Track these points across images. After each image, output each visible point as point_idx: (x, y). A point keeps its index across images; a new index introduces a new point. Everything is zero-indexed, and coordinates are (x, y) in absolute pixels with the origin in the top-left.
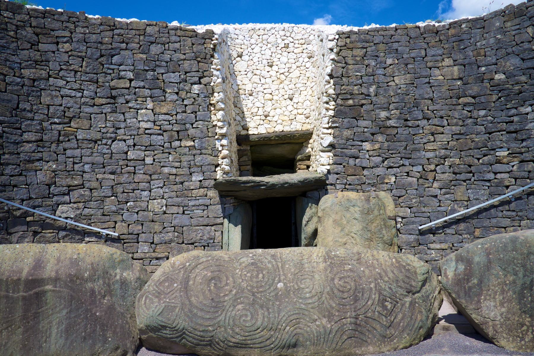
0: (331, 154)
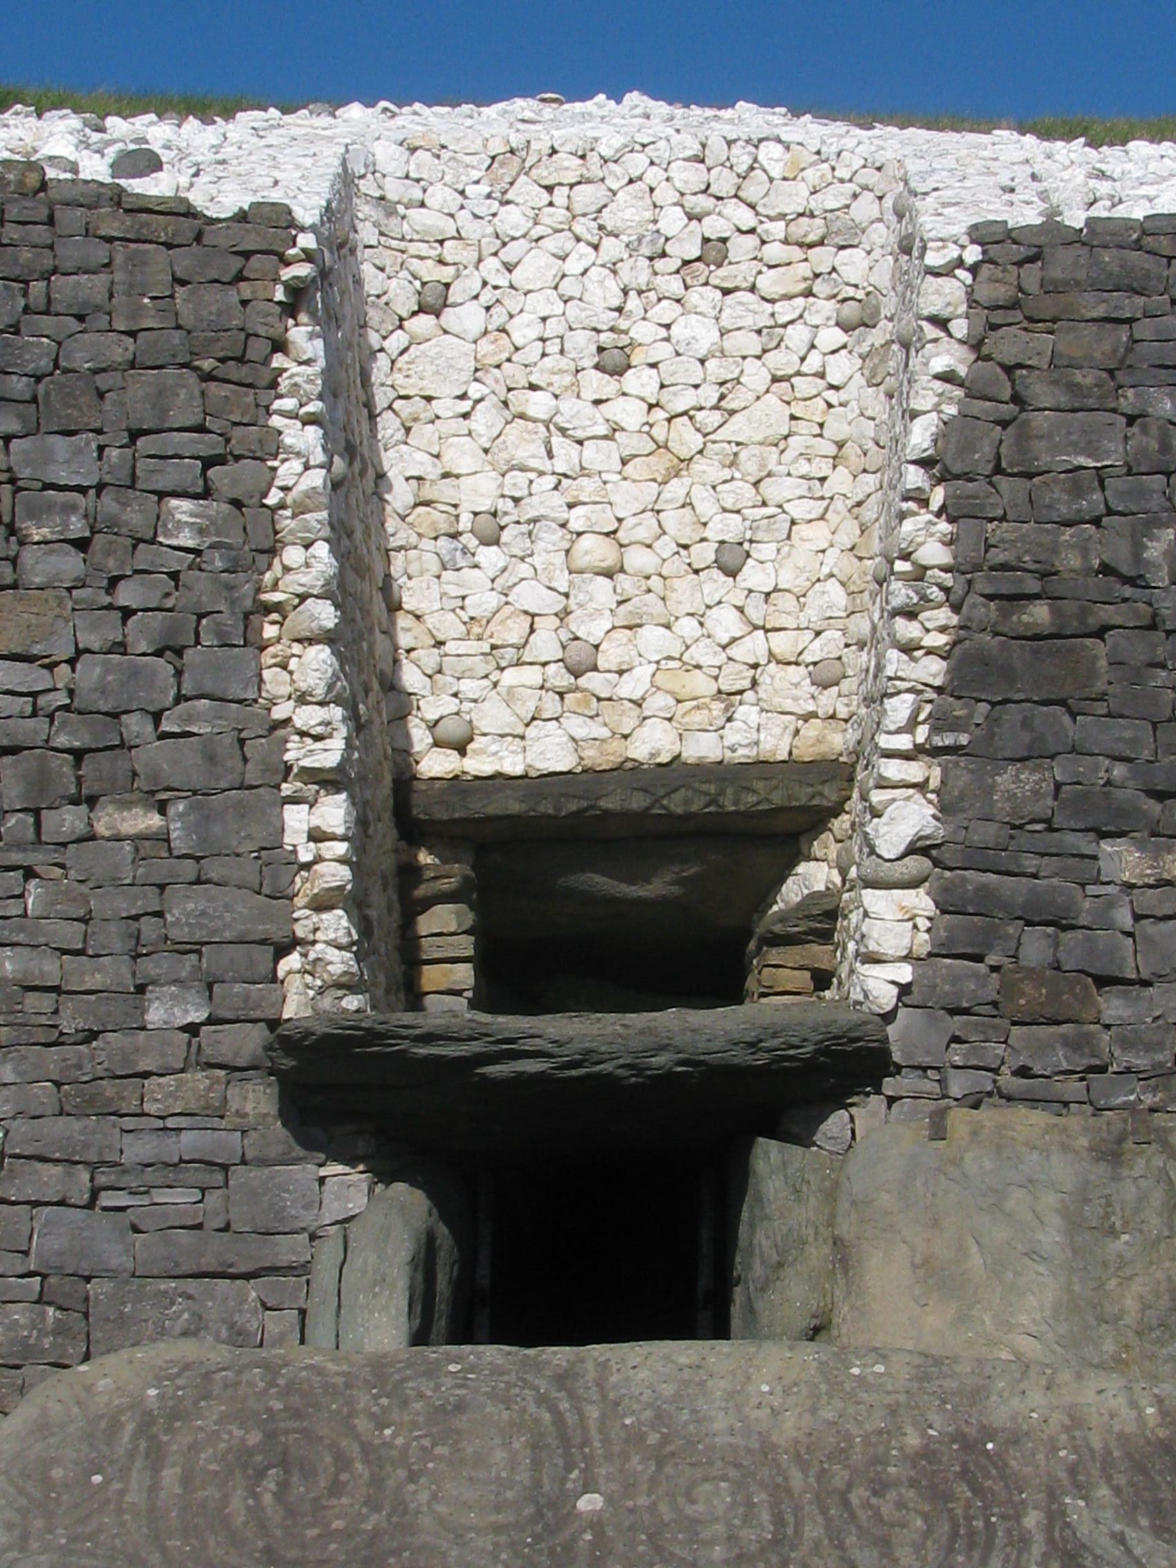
0: (921, 901)
